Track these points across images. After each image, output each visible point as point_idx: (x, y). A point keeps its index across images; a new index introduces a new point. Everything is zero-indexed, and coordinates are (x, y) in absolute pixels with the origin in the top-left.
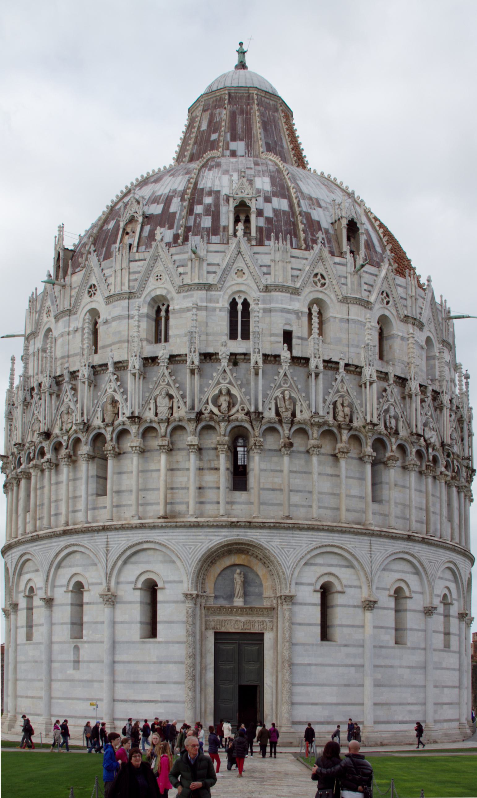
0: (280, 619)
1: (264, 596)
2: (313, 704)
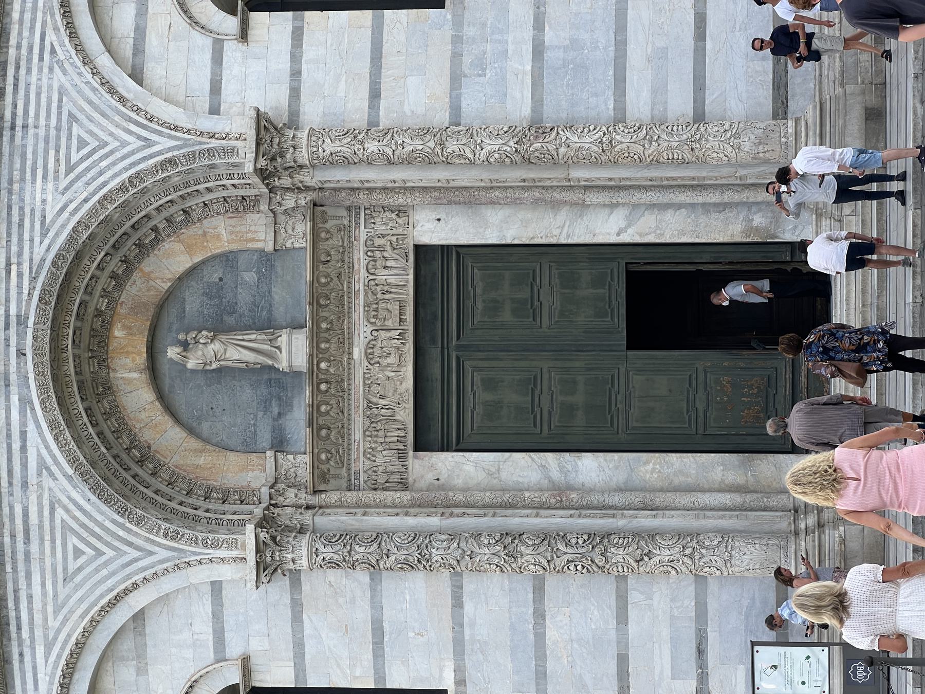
0: (357, 175)
1: (270, 247)
2: (700, 34)
